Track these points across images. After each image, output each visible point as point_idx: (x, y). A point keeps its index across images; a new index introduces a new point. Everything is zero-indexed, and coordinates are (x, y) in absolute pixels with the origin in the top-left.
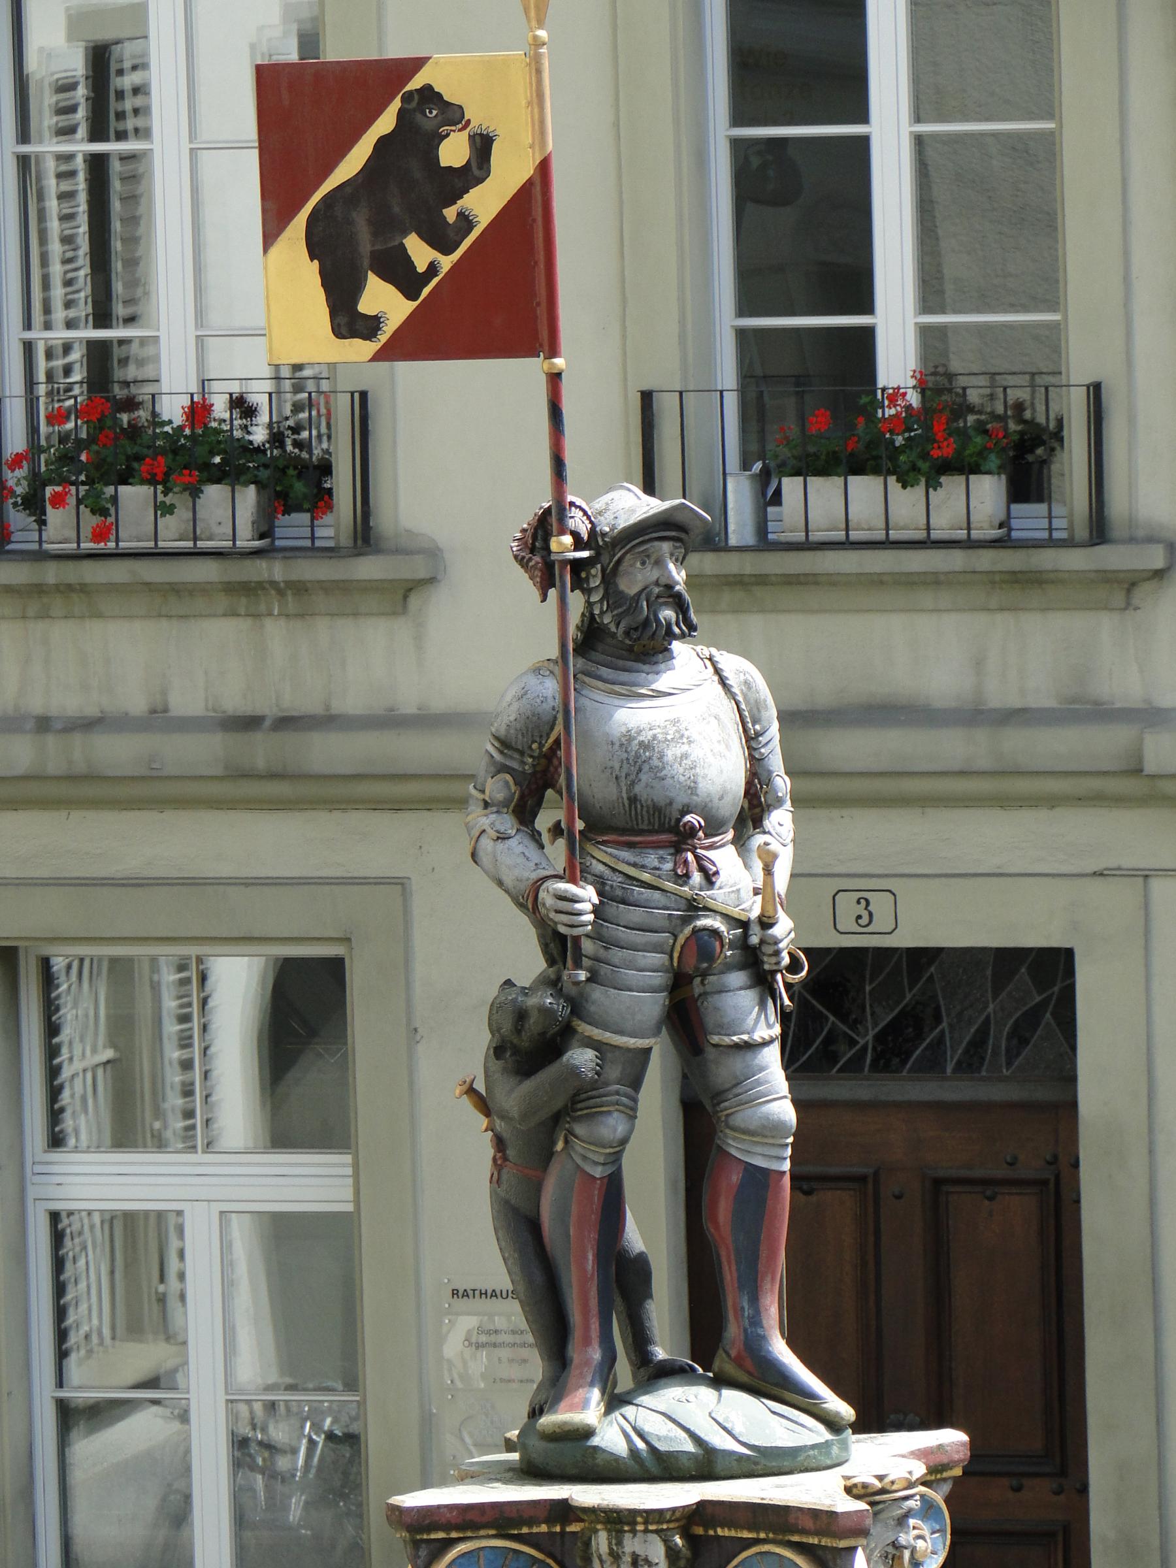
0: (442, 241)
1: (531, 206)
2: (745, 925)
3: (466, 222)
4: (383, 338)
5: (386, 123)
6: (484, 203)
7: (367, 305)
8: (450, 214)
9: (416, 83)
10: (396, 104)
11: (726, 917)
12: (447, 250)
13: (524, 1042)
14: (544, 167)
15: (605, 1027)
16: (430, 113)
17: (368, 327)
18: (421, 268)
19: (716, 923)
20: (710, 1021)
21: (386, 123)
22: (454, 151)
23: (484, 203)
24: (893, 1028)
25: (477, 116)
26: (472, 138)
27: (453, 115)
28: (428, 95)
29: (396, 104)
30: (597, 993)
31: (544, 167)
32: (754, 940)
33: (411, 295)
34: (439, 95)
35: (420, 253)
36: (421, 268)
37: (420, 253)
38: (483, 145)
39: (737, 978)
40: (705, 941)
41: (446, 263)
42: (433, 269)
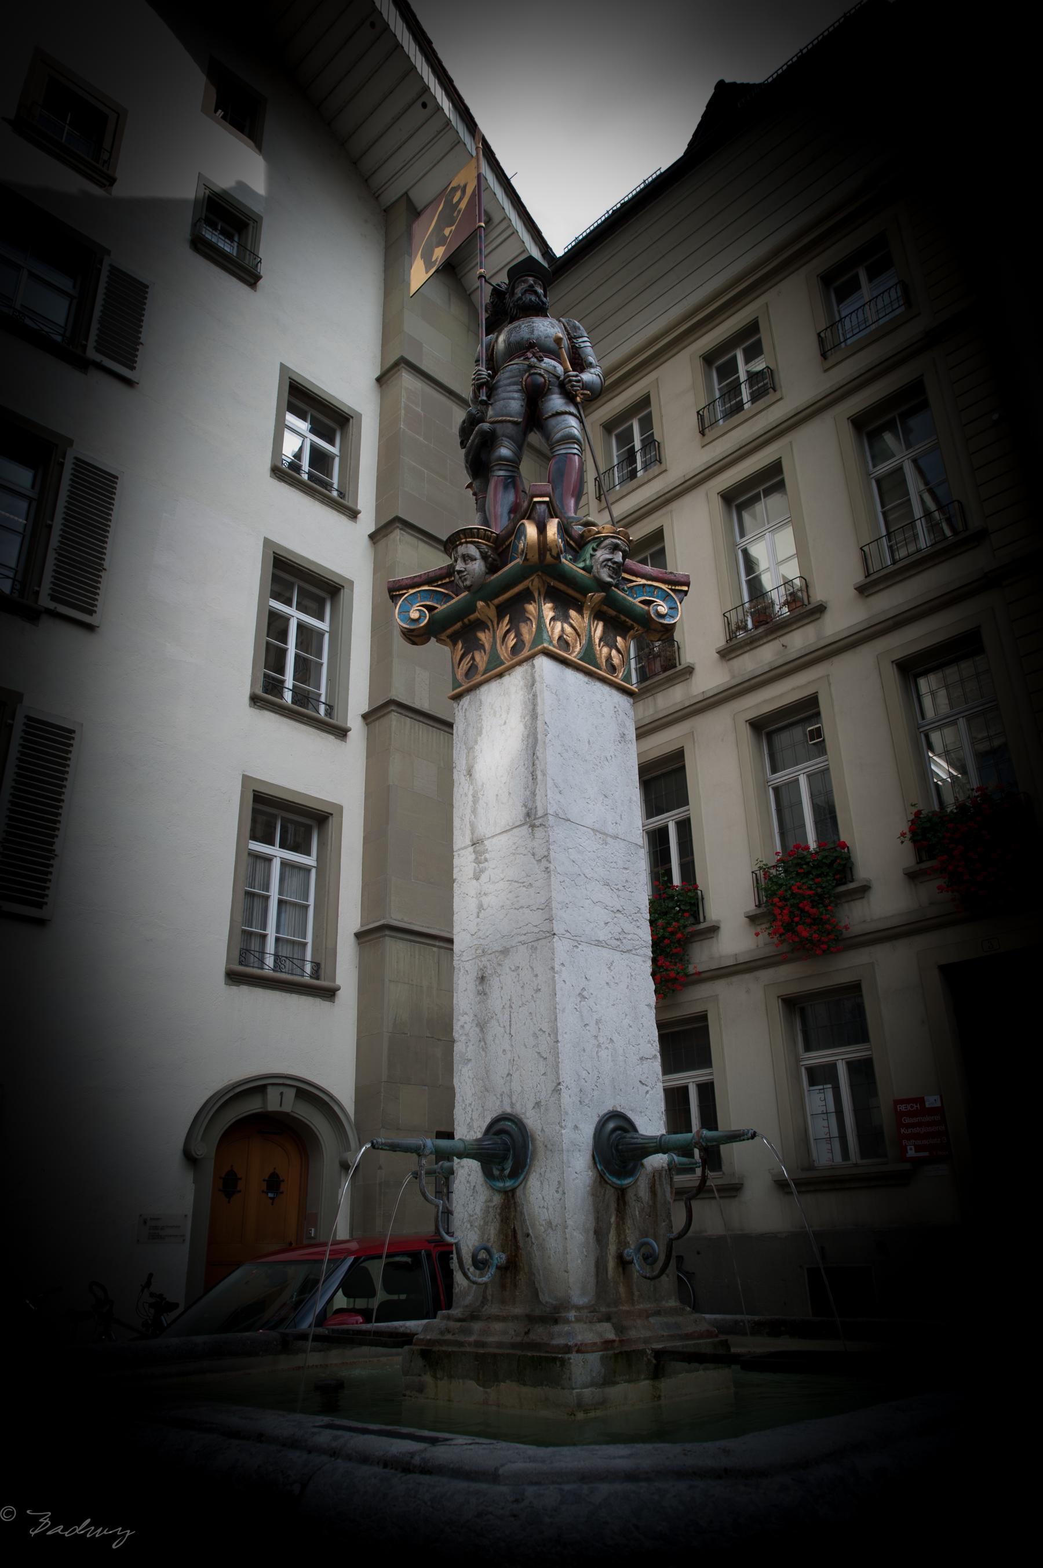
2: (558, 378)
19: (542, 372)
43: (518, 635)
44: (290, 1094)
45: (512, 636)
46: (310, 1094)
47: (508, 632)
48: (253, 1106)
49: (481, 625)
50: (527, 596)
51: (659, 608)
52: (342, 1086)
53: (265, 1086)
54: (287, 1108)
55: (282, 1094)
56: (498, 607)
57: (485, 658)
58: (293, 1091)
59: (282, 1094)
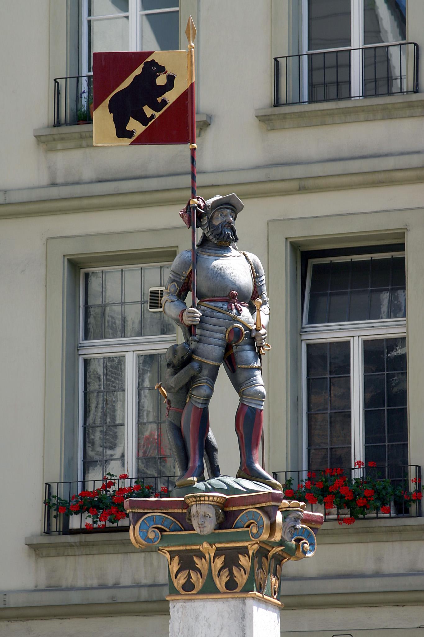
0: (156, 107)
1: (187, 97)
3: (164, 102)
4: (134, 138)
5: (138, 71)
6: (171, 97)
7: (129, 128)
8: (159, 100)
9: (149, 59)
10: (142, 65)
11: (244, 325)
12: (158, 111)
13: (175, 361)
14: (192, 85)
15: (202, 356)
16: (154, 69)
17: (130, 134)
18: (149, 116)
20: (238, 360)
21: (138, 71)
22: (161, 80)
23: (171, 97)
25: (170, 70)
26: (168, 77)
27: (162, 69)
29: (142, 65)
30: (201, 346)
31: (192, 85)
32: (253, 335)
33: (145, 124)
34: (157, 63)
35: (148, 111)
36: (149, 116)
37: (148, 111)
38: (171, 79)
39: (247, 347)
40: (238, 333)
41: (157, 115)
42: (153, 116)
43: (231, 573)
49: (201, 556)
51: (305, 545)
56: (218, 549)
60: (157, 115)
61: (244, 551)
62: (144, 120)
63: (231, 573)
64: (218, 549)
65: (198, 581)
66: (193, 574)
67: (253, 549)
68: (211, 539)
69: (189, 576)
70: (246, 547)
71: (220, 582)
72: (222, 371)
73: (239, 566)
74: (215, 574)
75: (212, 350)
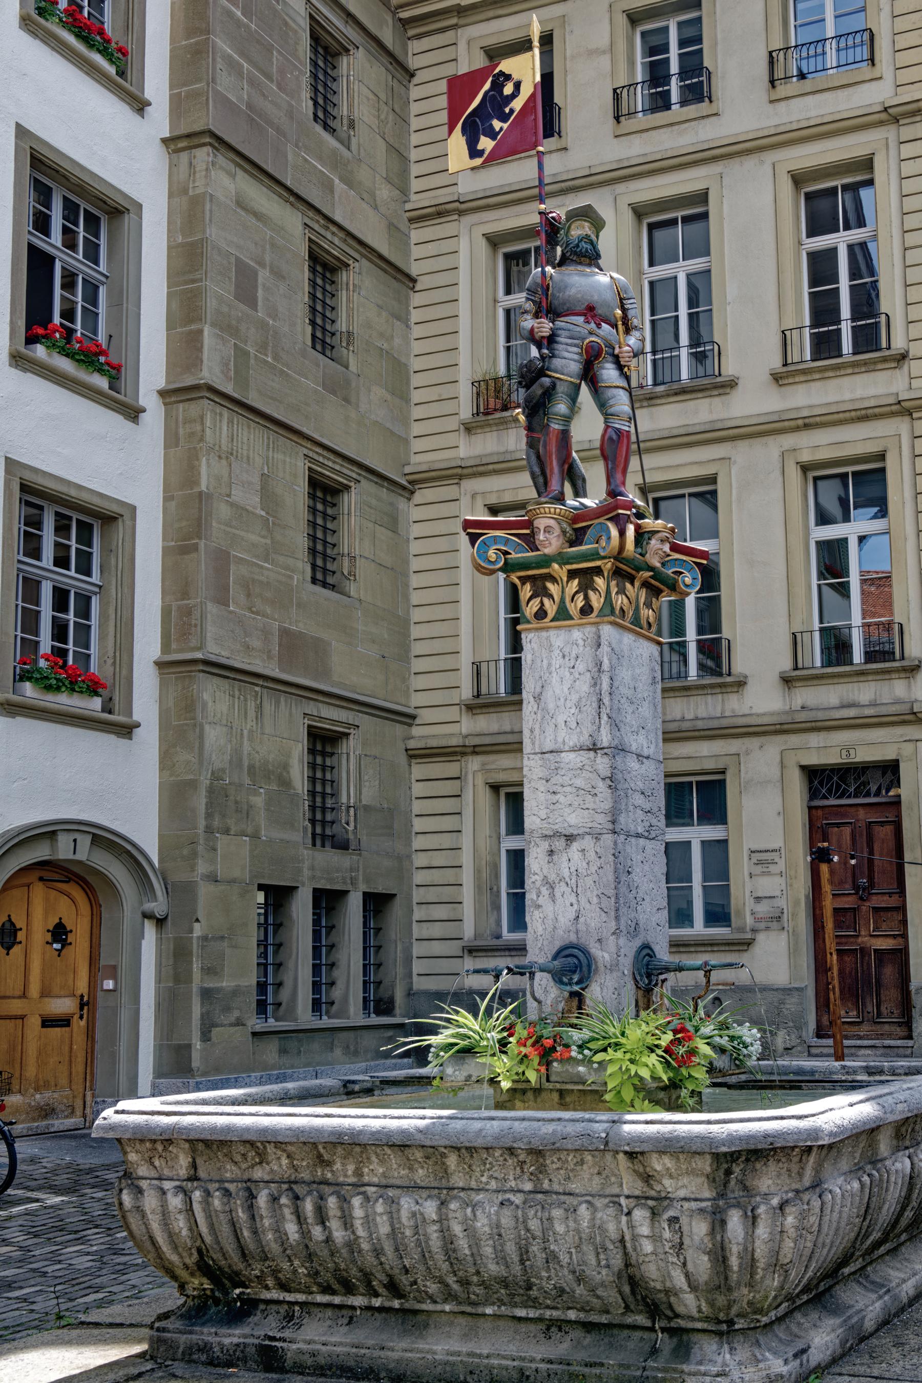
0: (504, 118)
9: (497, 71)
15: (556, 372)
17: (480, 153)
18: (497, 129)
22: (508, 89)
24: (859, 787)
28: (501, 73)
35: (497, 124)
36: (497, 129)
37: (497, 124)
41: (505, 126)
42: (501, 129)
43: (586, 597)
44: (85, 842)
45: (582, 597)
46: (105, 840)
47: (577, 593)
48: (41, 852)
49: (553, 580)
50: (598, 571)
52: (146, 836)
53: (54, 833)
54: (82, 855)
55: (75, 841)
56: (569, 571)
57: (555, 608)
58: (88, 839)
59: (75, 841)
60: (505, 126)
61: (598, 571)
62: (492, 134)
63: (586, 597)
64: (569, 571)
65: (551, 608)
66: (546, 601)
67: (607, 566)
68: (562, 559)
69: (542, 603)
70: (599, 567)
71: (574, 608)
72: (584, 388)
73: (595, 590)
74: (568, 600)
75: (568, 362)
